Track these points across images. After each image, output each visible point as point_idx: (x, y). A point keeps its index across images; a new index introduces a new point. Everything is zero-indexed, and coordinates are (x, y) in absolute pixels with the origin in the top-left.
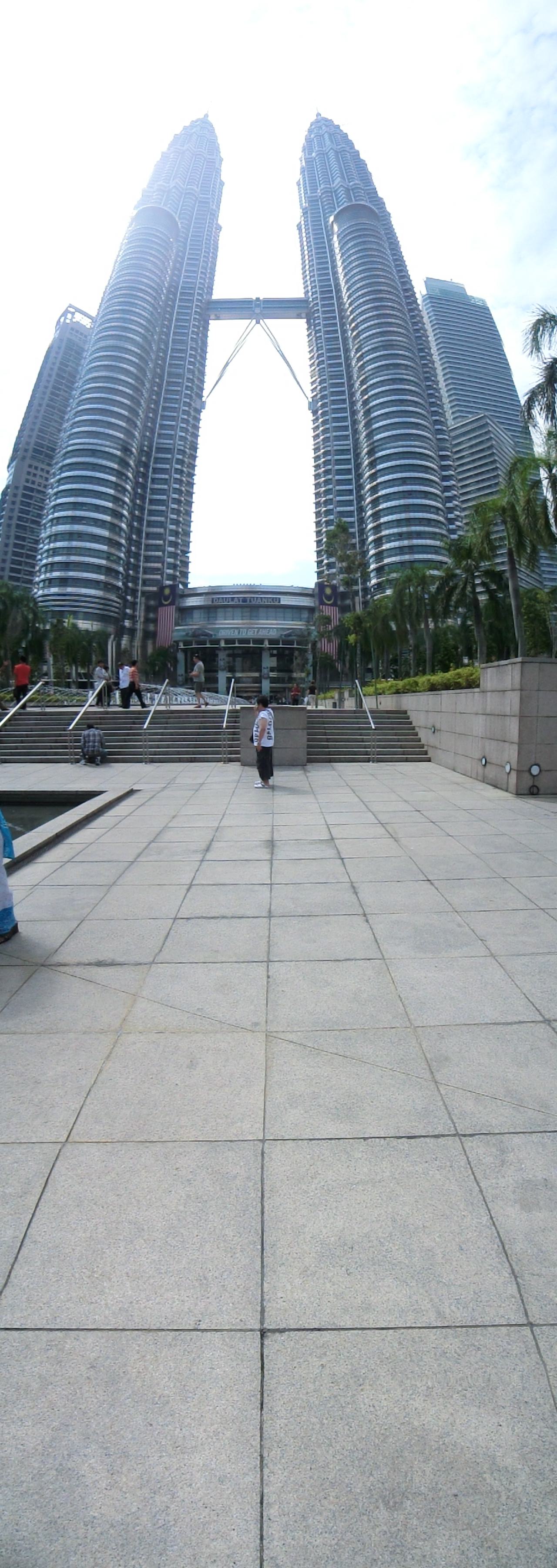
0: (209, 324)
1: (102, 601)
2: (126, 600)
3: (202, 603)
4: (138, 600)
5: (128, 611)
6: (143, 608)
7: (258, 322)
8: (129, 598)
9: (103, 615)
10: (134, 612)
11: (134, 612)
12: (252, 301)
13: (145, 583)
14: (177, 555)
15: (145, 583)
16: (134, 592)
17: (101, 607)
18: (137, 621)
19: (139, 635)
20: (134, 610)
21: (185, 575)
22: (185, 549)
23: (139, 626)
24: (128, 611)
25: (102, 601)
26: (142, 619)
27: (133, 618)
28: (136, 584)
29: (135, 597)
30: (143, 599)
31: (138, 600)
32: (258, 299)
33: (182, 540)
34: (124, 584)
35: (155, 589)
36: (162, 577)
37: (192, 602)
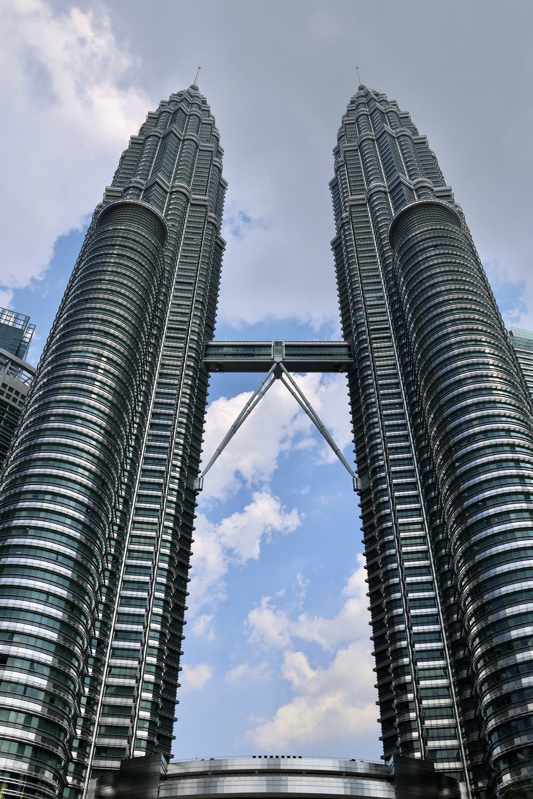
2: (64, 784)
4: (84, 786)
7: (278, 375)
8: (69, 779)
12: (270, 346)
29: (79, 777)
31: (84, 786)
32: (277, 343)
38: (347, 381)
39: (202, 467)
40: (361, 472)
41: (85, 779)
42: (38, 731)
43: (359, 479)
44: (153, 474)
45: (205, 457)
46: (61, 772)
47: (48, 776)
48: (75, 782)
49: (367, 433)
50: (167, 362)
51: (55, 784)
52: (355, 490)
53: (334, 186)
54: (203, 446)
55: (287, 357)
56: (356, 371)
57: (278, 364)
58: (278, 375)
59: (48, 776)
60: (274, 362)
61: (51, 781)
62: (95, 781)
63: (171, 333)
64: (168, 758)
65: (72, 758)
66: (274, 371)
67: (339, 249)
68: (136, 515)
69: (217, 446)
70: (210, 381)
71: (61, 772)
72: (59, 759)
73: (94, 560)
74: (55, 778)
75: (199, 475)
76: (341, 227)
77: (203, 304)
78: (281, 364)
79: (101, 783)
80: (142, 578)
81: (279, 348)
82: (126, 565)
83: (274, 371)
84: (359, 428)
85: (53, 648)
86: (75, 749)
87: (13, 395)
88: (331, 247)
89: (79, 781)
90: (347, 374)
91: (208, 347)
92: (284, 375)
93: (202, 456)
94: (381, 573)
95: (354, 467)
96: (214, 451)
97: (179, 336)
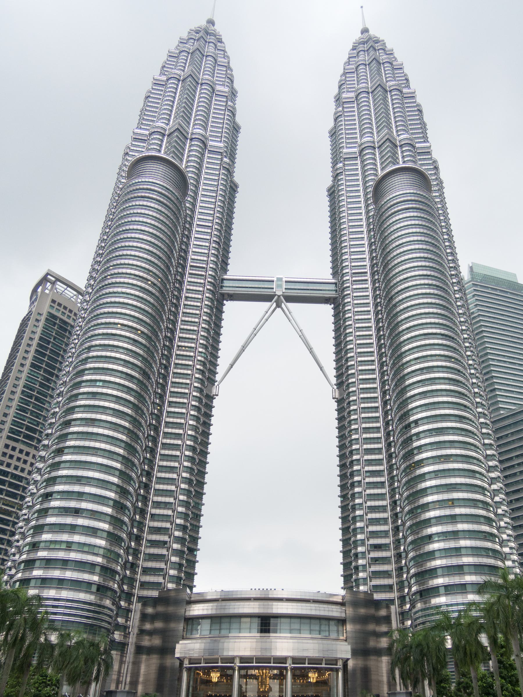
0: (223, 305)
1: (92, 608)
2: (119, 607)
3: (209, 612)
4: (133, 607)
5: (120, 620)
6: (138, 616)
8: (122, 603)
9: (91, 625)
10: (126, 621)
11: (126, 621)
12: (273, 281)
13: (144, 585)
14: (184, 552)
15: (144, 585)
16: (129, 596)
17: (91, 614)
18: (129, 633)
19: (131, 649)
20: (127, 619)
21: (190, 576)
22: (192, 546)
23: (132, 640)
24: (120, 620)
25: (92, 608)
26: (136, 631)
27: (124, 628)
28: (132, 586)
29: (130, 603)
30: (140, 604)
31: (133, 607)
33: (190, 536)
34: (119, 587)
35: (155, 594)
36: (164, 579)
37: (197, 610)
38: (332, 312)
39: (218, 377)
40: (340, 385)
41: (133, 602)
42: (100, 575)
43: (337, 390)
44: (180, 385)
45: (221, 370)
46: (117, 600)
47: (108, 602)
48: (127, 605)
49: (344, 347)
50: (190, 295)
51: (114, 608)
52: (333, 398)
53: (334, 134)
54: (219, 361)
55: (287, 291)
56: (339, 305)
57: (279, 296)
58: (279, 305)
59: (108, 602)
60: (276, 295)
61: (110, 606)
62: (140, 604)
63: (193, 270)
64: (191, 588)
65: (124, 590)
66: (275, 302)
67: (332, 196)
68: (168, 417)
69: (230, 361)
70: (225, 308)
71: (117, 600)
72: (115, 592)
73: (137, 455)
74: (113, 604)
75: (216, 384)
76: (336, 177)
77: (219, 244)
78: (282, 298)
79: (144, 605)
80: (172, 464)
81: (279, 283)
82: (160, 455)
83: (275, 302)
84: (338, 336)
85: (108, 519)
86: (125, 584)
87: (67, 312)
88: (327, 193)
89: (129, 604)
90: (333, 306)
91: (223, 280)
92: (283, 305)
93: (218, 369)
94: (347, 451)
95: (334, 381)
96: (227, 366)
97: (200, 273)
